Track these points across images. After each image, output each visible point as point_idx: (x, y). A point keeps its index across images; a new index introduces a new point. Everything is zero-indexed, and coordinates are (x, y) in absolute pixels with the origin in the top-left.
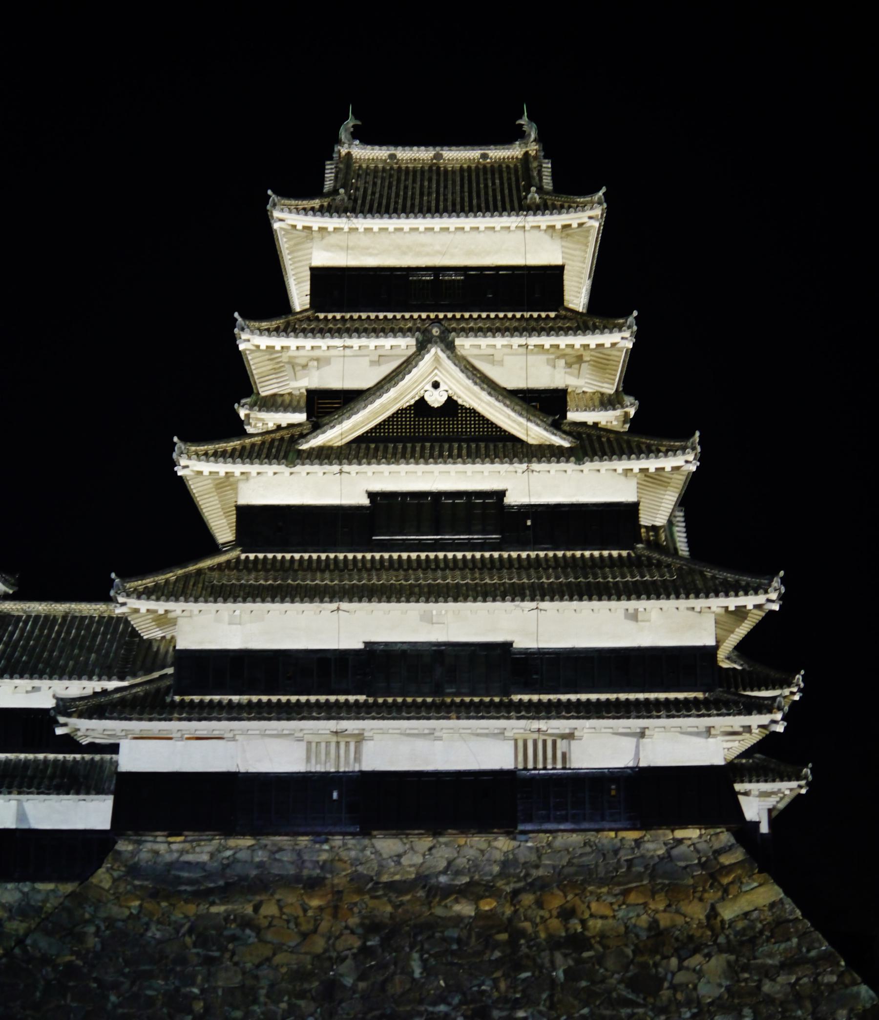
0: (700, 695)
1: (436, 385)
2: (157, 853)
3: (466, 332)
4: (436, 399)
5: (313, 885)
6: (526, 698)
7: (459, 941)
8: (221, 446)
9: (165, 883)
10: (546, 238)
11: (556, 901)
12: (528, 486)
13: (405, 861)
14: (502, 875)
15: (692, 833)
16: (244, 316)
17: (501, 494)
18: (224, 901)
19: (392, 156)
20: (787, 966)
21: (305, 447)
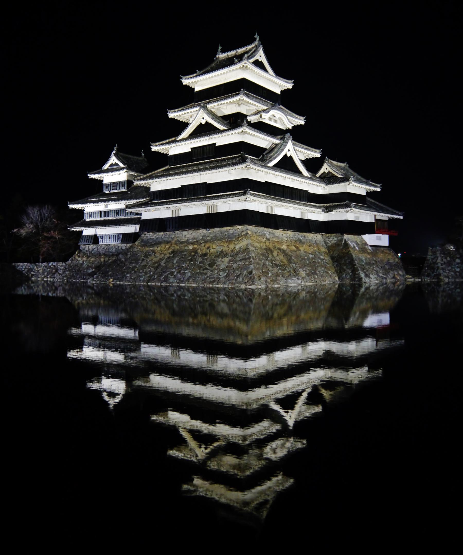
0: (242, 191)
1: (203, 118)
2: (147, 237)
3: (209, 103)
4: (203, 122)
5: (168, 242)
6: (209, 195)
7: (185, 255)
8: (163, 142)
9: (146, 243)
10: (240, 71)
11: (207, 246)
12: (220, 140)
13: (186, 237)
14: (202, 239)
15: (240, 227)
16: (169, 110)
17: (215, 144)
18: (153, 247)
19: (228, 55)
20: (241, 260)
21: (178, 139)
